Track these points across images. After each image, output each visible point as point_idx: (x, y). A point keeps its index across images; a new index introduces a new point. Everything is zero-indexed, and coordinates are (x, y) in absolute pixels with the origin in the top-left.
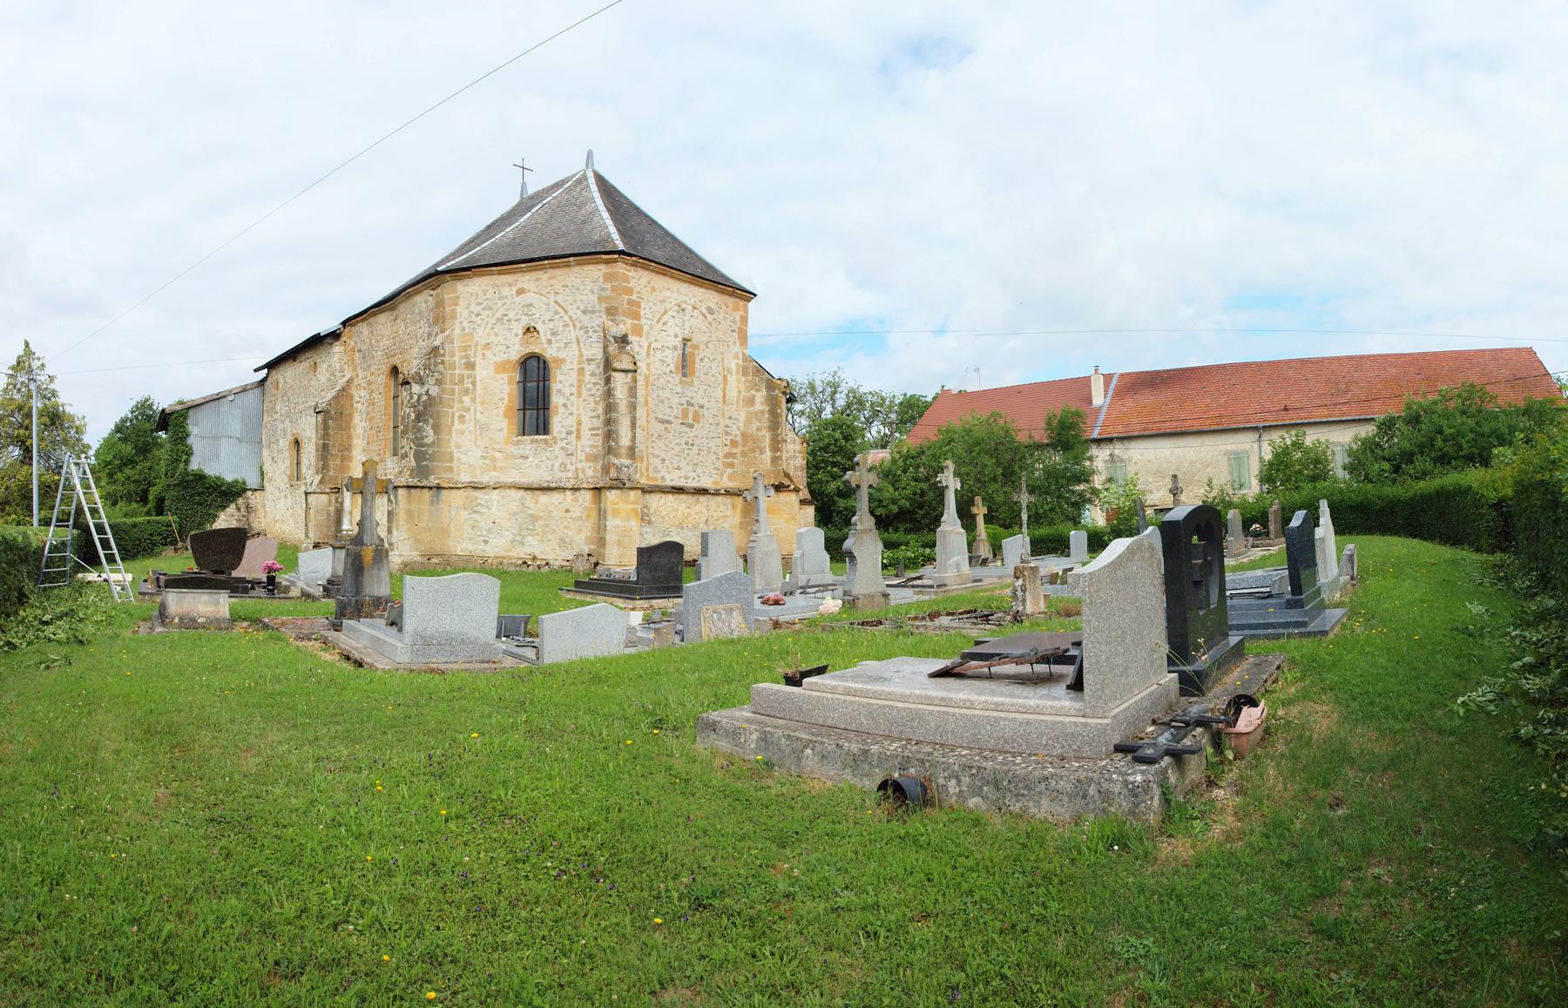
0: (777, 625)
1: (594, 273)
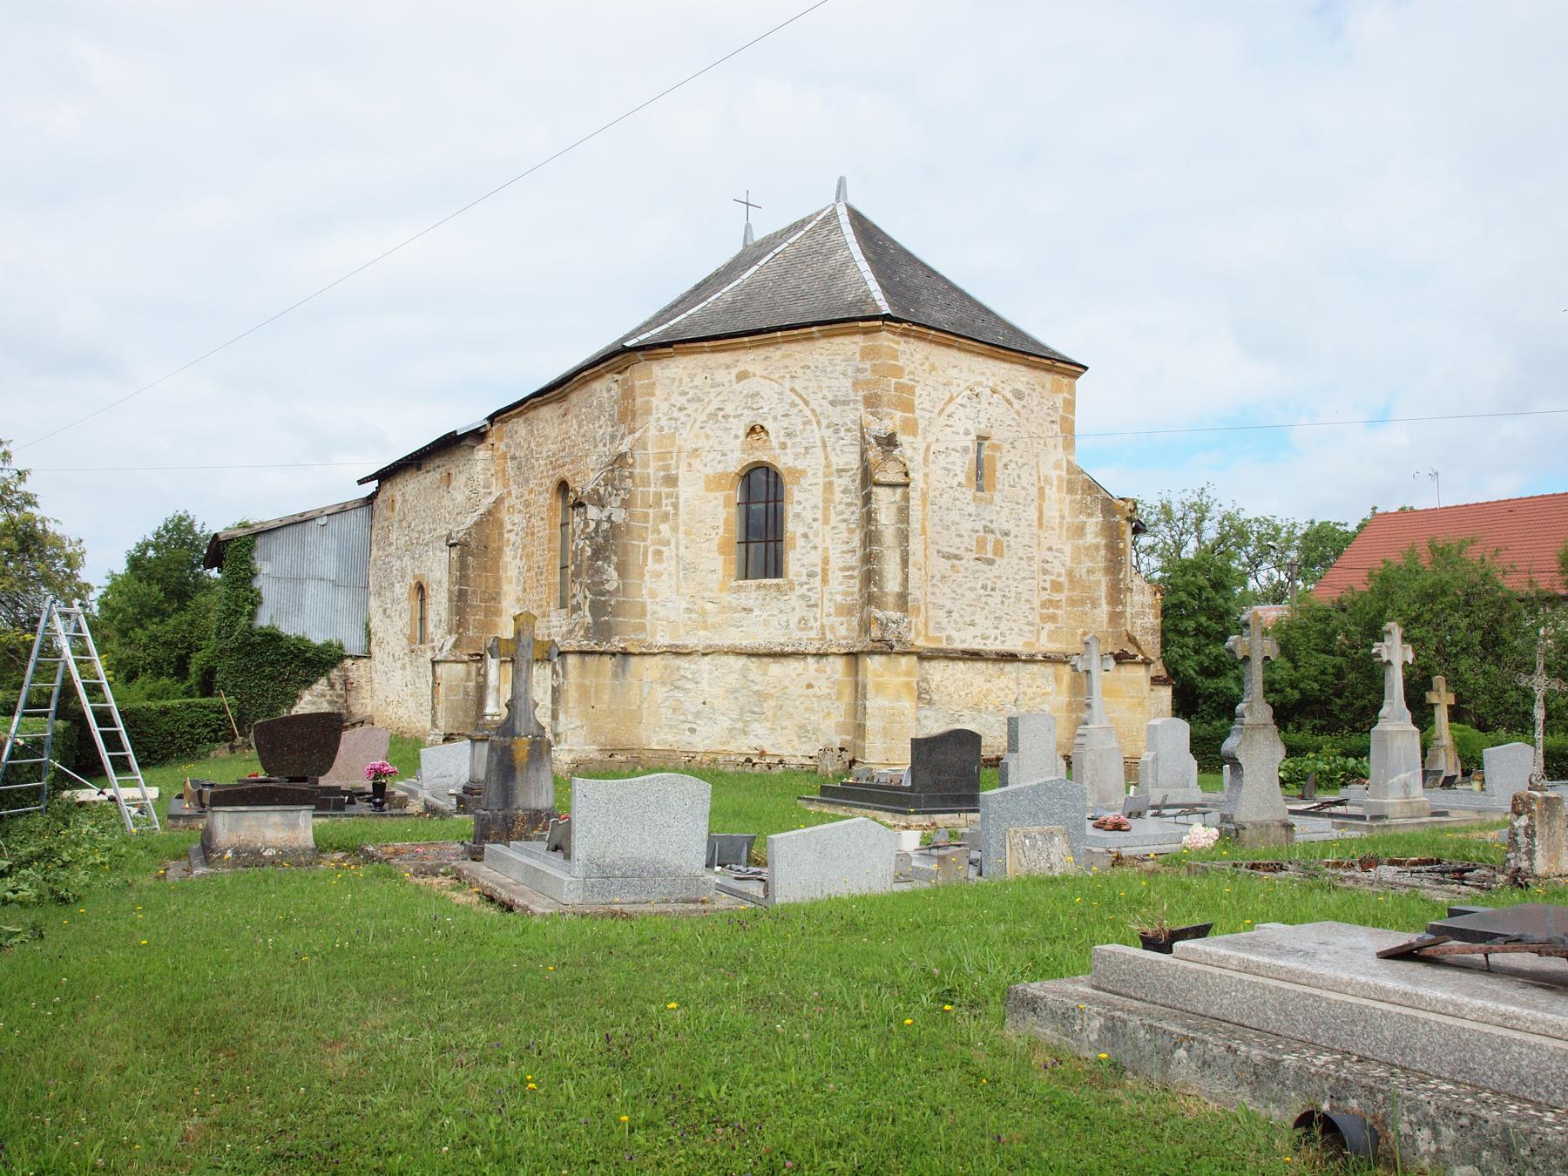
0: (1118, 860)
1: (849, 346)
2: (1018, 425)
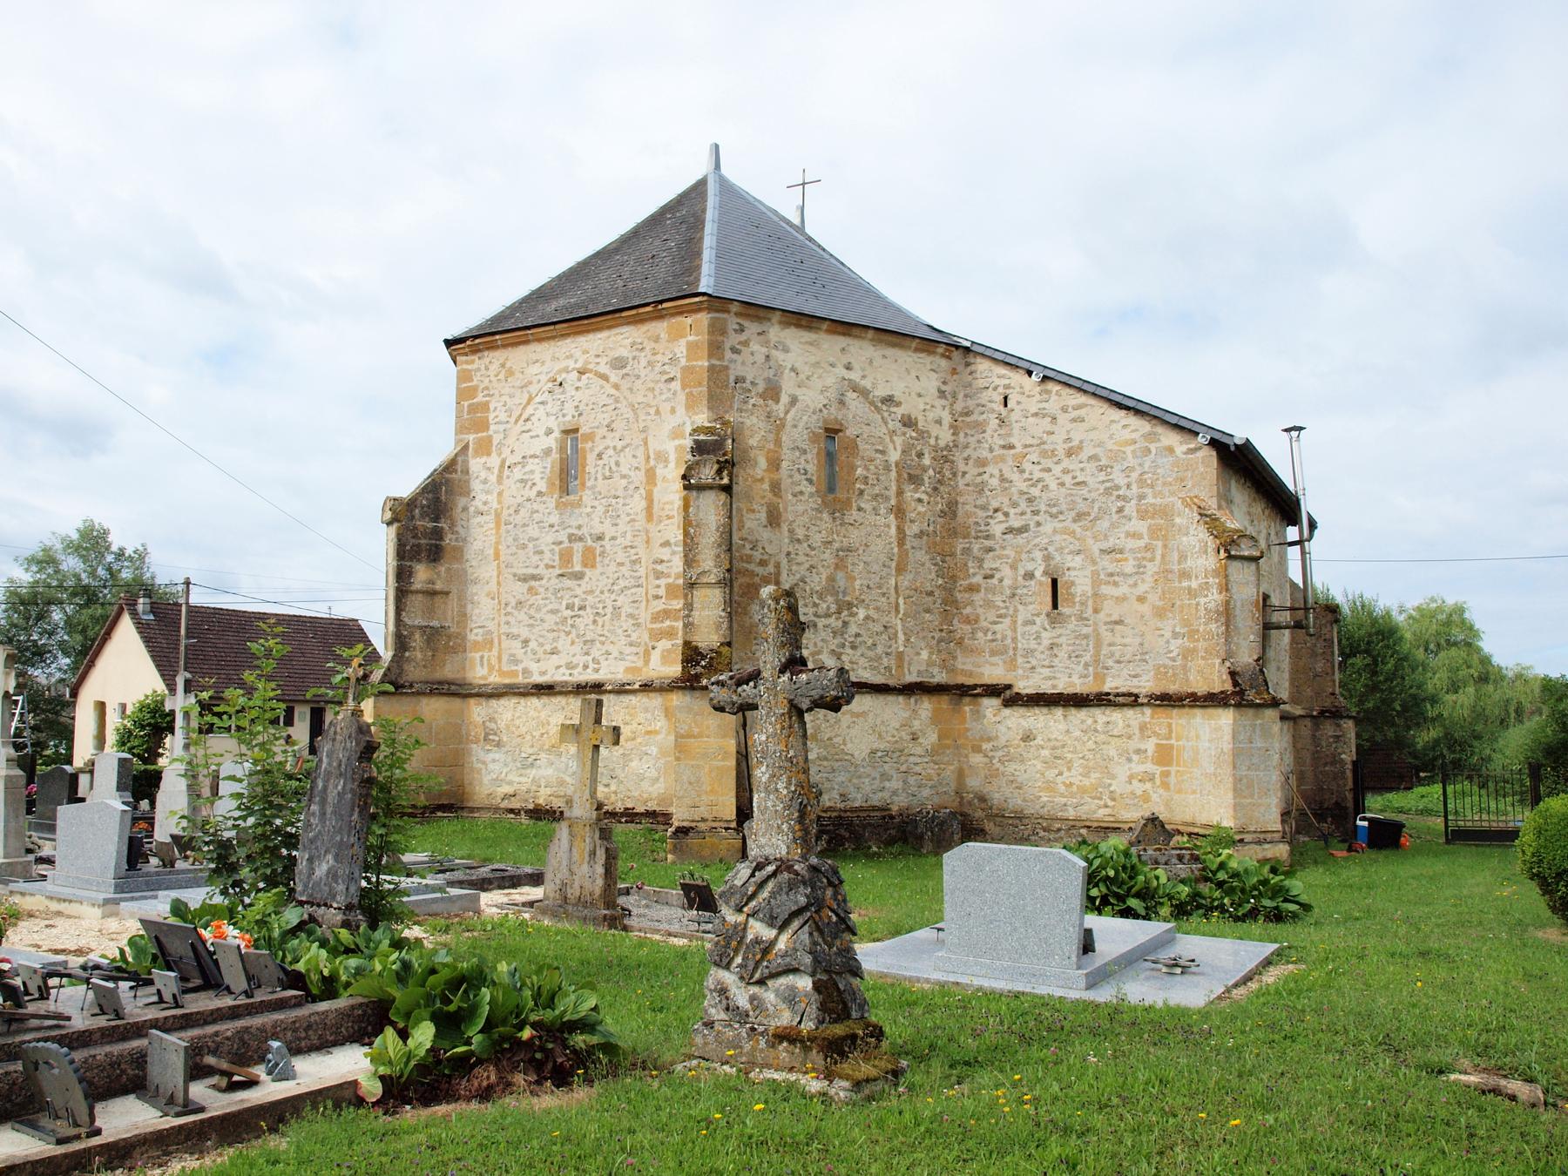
2: (617, 401)
